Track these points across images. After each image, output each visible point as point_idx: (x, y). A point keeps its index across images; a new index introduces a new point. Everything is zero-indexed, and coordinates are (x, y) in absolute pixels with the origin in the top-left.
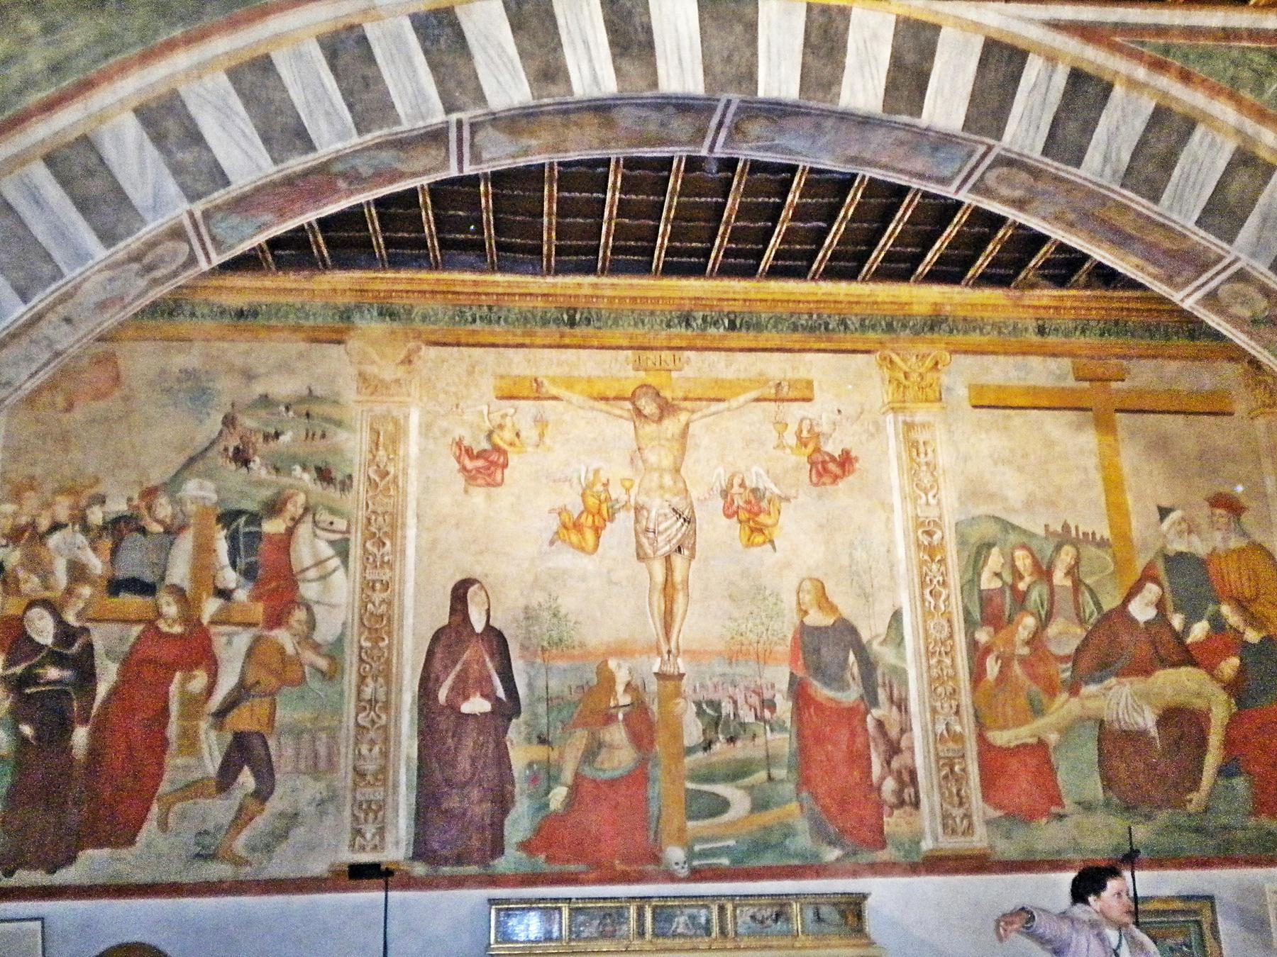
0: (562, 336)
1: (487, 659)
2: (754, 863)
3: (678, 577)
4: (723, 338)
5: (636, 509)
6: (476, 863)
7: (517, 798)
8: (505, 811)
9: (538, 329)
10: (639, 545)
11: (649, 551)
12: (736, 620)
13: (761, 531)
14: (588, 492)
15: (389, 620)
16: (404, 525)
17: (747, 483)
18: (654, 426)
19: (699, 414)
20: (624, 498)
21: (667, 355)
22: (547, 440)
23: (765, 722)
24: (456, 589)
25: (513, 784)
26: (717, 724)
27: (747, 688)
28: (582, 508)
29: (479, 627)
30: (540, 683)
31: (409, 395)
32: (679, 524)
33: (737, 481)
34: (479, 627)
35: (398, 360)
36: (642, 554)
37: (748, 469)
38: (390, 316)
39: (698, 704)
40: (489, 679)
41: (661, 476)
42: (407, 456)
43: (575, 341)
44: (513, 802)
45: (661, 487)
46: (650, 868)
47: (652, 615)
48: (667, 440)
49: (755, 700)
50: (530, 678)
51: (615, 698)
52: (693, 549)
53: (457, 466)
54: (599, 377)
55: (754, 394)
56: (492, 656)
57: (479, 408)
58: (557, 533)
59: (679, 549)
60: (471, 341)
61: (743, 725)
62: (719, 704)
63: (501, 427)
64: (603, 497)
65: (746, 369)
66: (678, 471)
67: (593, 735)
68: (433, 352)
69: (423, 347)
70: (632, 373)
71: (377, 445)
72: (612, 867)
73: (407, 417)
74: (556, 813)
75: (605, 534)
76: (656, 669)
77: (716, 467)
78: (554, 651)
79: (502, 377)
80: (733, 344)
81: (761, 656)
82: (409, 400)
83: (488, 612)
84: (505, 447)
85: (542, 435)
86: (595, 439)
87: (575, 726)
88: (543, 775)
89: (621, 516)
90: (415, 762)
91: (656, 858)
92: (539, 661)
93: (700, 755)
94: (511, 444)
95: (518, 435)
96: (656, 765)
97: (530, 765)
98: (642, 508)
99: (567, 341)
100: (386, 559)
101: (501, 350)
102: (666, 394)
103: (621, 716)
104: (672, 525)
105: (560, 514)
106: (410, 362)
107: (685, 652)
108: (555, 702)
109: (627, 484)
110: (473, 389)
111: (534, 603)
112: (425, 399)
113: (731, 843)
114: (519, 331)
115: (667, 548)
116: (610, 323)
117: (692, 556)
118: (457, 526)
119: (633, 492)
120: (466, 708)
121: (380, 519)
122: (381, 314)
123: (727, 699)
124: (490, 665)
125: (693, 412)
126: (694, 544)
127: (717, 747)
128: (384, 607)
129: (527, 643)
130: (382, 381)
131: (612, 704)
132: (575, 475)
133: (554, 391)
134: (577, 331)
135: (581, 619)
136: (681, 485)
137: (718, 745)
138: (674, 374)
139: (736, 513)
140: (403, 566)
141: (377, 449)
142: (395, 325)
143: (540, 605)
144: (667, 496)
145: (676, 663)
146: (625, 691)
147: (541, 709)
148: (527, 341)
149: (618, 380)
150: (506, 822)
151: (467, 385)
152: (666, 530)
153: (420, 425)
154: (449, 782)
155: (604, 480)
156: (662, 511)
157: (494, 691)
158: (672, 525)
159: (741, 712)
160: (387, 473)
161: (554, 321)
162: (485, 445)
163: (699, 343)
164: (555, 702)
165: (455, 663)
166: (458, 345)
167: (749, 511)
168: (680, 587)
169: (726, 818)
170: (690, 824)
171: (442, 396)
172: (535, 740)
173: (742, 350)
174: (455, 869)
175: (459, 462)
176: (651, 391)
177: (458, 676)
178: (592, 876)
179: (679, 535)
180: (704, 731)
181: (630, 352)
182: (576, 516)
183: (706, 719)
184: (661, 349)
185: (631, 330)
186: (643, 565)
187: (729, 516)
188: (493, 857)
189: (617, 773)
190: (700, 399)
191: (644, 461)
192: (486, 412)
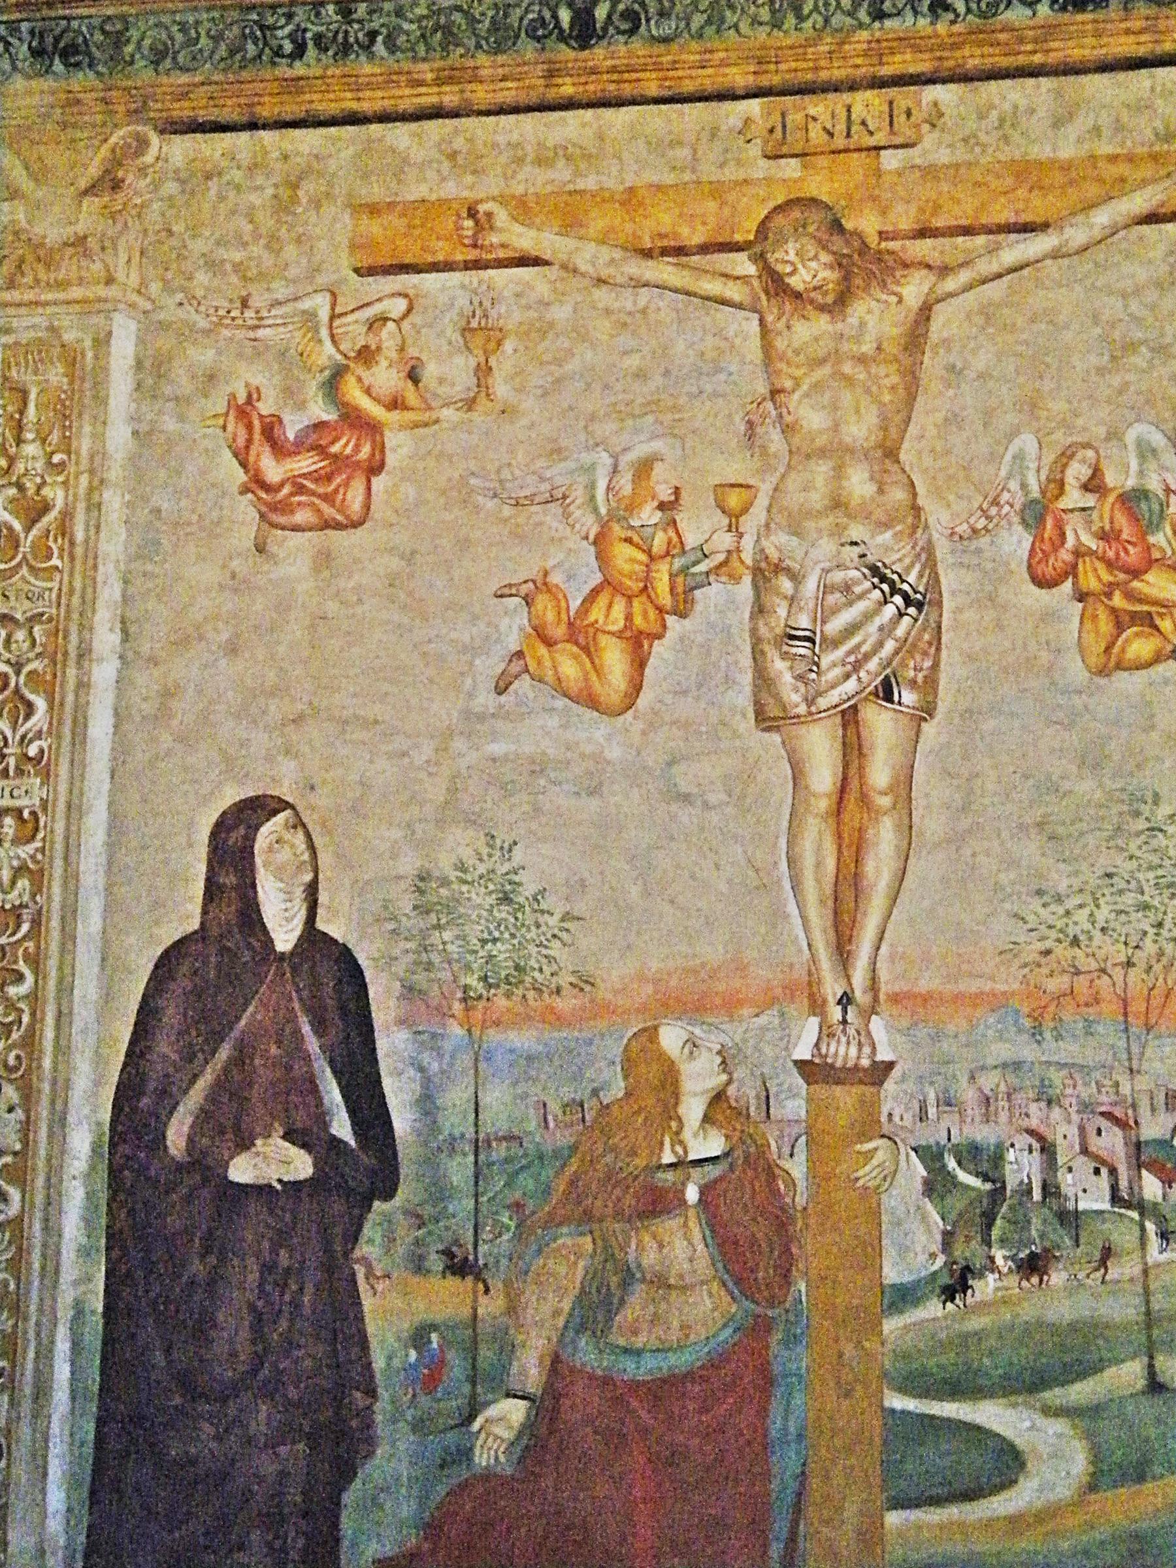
0: (551, 74)
1: (306, 1029)
3: (880, 774)
4: (1049, 30)
5: (757, 571)
7: (382, 1428)
8: (345, 1472)
9: (482, 59)
10: (763, 680)
11: (794, 698)
12: (1059, 899)
13: (1148, 621)
14: (617, 530)
15: (36, 923)
16: (84, 653)
17: (1111, 478)
18: (823, 323)
19: (964, 276)
20: (726, 540)
21: (869, 104)
22: (501, 389)
23: (1141, 1206)
24: (221, 828)
25: (372, 1393)
26: (989, 1219)
27: (1086, 1107)
28: (597, 578)
29: (285, 939)
30: (456, 1097)
31: (110, 281)
32: (890, 610)
33: (1077, 472)
34: (285, 939)
35: (83, 184)
36: (773, 711)
37: (1114, 435)
38: (65, 55)
39: (931, 1156)
40: (312, 1087)
41: (839, 472)
42: (99, 454)
43: (593, 89)
44: (371, 1442)
45: (837, 503)
47: (796, 887)
48: (862, 360)
49: (1112, 1142)
50: (427, 1081)
51: (677, 1139)
52: (930, 684)
53: (241, 476)
54: (659, 188)
55: (1139, 202)
56: (320, 1027)
57: (306, 304)
58: (519, 654)
59: (886, 692)
60: (292, 110)
61: (1071, 1219)
62: (998, 1158)
63: (366, 355)
64: (659, 542)
65: (1119, 127)
66: (891, 453)
67: (608, 1254)
68: (181, 148)
69: (154, 139)
70: (762, 168)
71: (20, 427)
73: (102, 342)
74: (487, 1476)
75: (660, 652)
76: (803, 1052)
77: (1015, 432)
78: (501, 1002)
79: (374, 210)
80: (1077, 52)
81: (1137, 1007)
82: (113, 292)
83: (312, 890)
84: (376, 411)
85: (483, 371)
86: (641, 375)
87: (552, 1222)
88: (456, 1366)
89: (710, 597)
90: (95, 1323)
92: (456, 1030)
93: (933, 1309)
94: (395, 404)
95: (413, 376)
96: (792, 1340)
97: (419, 1337)
98: (778, 568)
99: (567, 89)
100: (32, 751)
101: (375, 128)
102: (867, 223)
103: (692, 1194)
104: (868, 617)
105: (528, 601)
106: (117, 186)
107: (895, 999)
108: (500, 1151)
109: (734, 500)
110: (290, 251)
111: (445, 865)
112: (155, 288)
114: (426, 71)
115: (851, 686)
116: (698, 20)
117: (927, 711)
118: (232, 649)
119: (751, 523)
120: (241, 1171)
121: (20, 635)
122: (37, 53)
123: (1024, 1140)
124: (313, 1044)
125: (945, 271)
126: (936, 666)
127: (985, 1287)
128: (23, 883)
129: (420, 978)
130: (36, 246)
131: (668, 1158)
132: (582, 479)
133: (525, 240)
134: (598, 54)
135: (579, 908)
136: (899, 495)
137: (991, 1278)
138: (891, 160)
139: (1071, 571)
140: (78, 766)
141: (19, 441)
142: (82, 80)
143: (462, 867)
144: (856, 531)
145: (866, 1038)
146: (707, 1119)
147: (459, 1170)
148: (450, 97)
149: (717, 191)
150: (348, 1498)
151: (273, 244)
152: (851, 630)
153: (139, 365)
154: (185, 1382)
155: (665, 494)
156: (838, 577)
157: (322, 1118)
158: (868, 617)
159: (1067, 1182)
160: (45, 508)
161: (532, 35)
162: (326, 413)
163: (974, 58)
164: (500, 1151)
165: (216, 1038)
166: (253, 126)
167: (1110, 565)
168: (885, 801)
169: (1001, 1505)
170: (893, 1519)
171: (202, 277)
172: (436, 1263)
173: (1104, 67)
175: (244, 465)
176: (815, 217)
177: (219, 1085)
179: (890, 646)
180: (948, 1240)
181: (754, 106)
182: (575, 604)
183: (957, 1203)
184: (853, 86)
185: (762, 33)
186: (776, 738)
187: (1041, 582)
189: (680, 1361)
190: (967, 231)
191: (788, 430)
192: (324, 315)
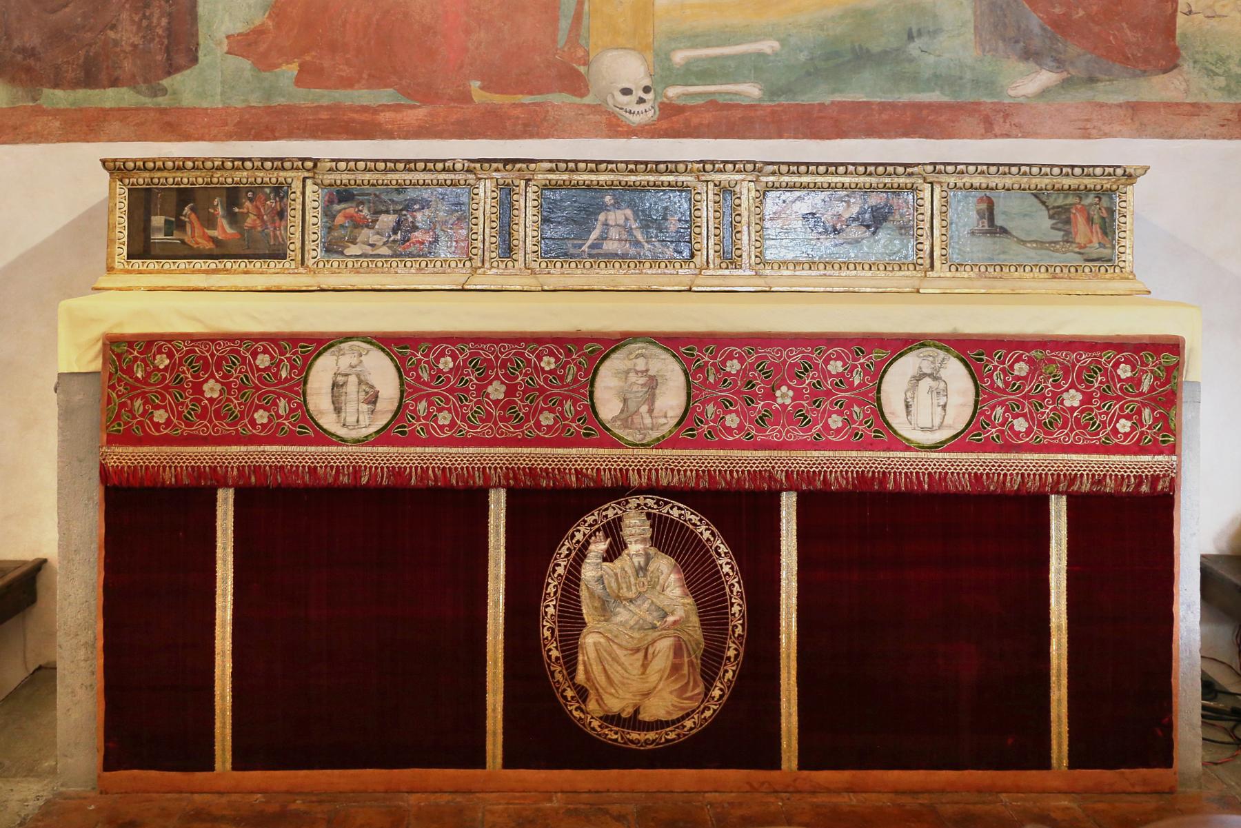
2: (821, 95)
6: (132, 82)
46: (558, 99)
72: (466, 98)
91: (574, 82)
113: (768, 46)
174: (81, 93)
178: (419, 114)
188: (172, 69)
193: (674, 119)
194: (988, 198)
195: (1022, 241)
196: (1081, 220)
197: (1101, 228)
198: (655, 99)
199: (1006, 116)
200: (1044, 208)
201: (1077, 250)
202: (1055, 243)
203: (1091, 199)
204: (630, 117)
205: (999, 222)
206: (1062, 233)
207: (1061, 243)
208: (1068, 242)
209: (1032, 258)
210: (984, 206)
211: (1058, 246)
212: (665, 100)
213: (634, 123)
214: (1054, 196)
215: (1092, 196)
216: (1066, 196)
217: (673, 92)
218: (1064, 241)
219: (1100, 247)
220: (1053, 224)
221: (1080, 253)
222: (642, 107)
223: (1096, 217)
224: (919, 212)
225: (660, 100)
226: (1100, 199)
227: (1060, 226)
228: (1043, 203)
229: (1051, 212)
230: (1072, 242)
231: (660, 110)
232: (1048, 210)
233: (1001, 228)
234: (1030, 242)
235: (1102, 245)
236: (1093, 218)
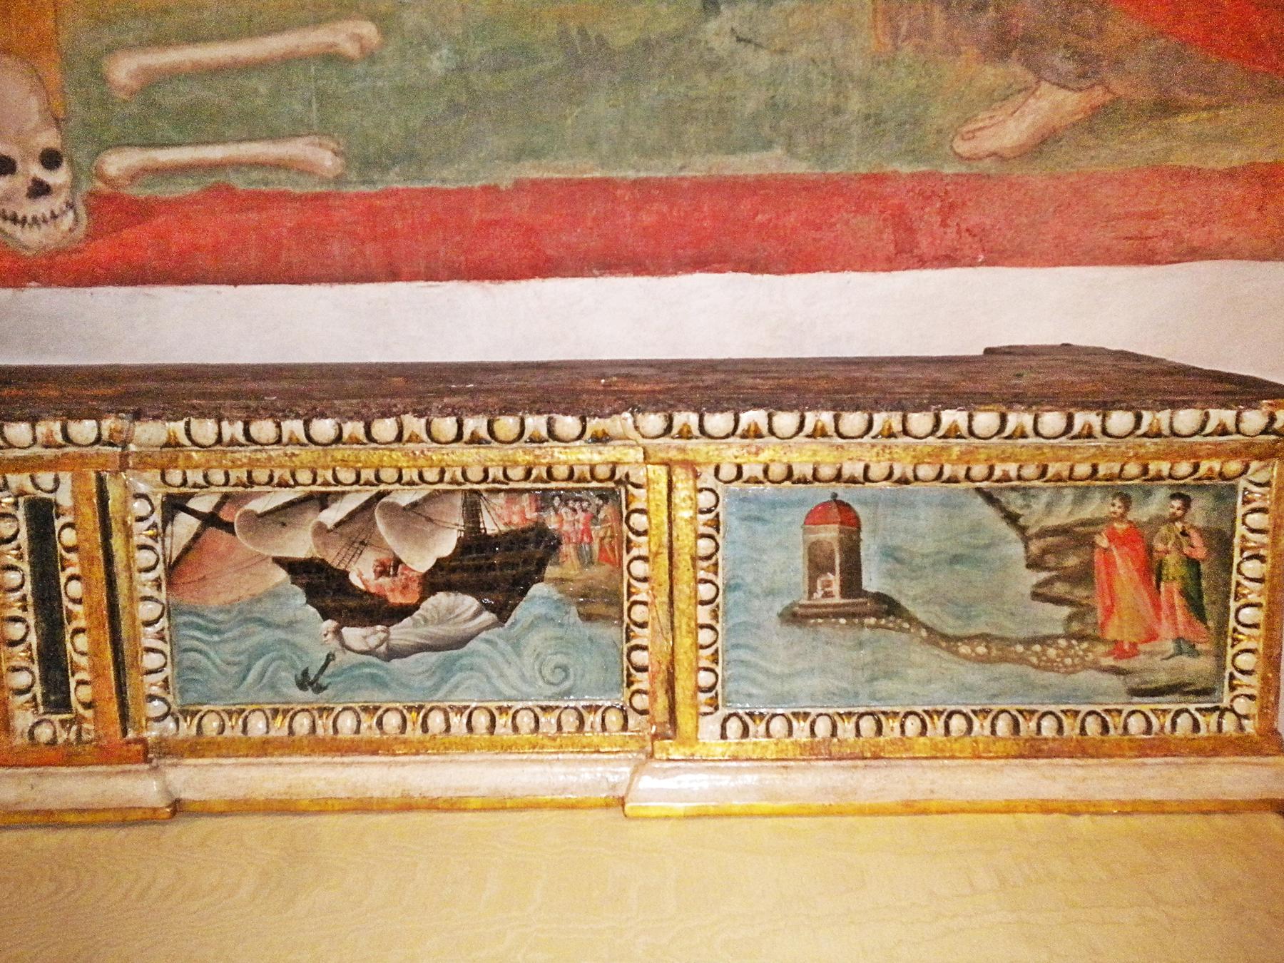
193: (128, 235)
194: (844, 507)
195: (945, 637)
196: (1125, 570)
197: (1184, 593)
198: (74, 185)
199: (949, 210)
200: (1013, 534)
201: (1109, 662)
202: (1045, 640)
203: (1158, 504)
204: (16, 230)
205: (872, 581)
206: (1066, 611)
207: (1063, 643)
208: (1081, 638)
209: (971, 688)
210: (830, 534)
211: (1052, 652)
212: (99, 184)
213: (27, 248)
214: (1044, 498)
215: (1161, 494)
216: (1082, 496)
217: (117, 163)
218: (1069, 636)
219: (1180, 652)
220: (1039, 585)
221: (1117, 671)
222: (42, 207)
223: (1172, 560)
224: (635, 552)
225: (86, 187)
226: (1187, 502)
227: (1060, 589)
228: (1012, 519)
229: (1035, 547)
230: (1098, 639)
231: (89, 214)
232: (1026, 540)
233: (880, 598)
234: (969, 639)
235: (1185, 647)
236: (1161, 565)
